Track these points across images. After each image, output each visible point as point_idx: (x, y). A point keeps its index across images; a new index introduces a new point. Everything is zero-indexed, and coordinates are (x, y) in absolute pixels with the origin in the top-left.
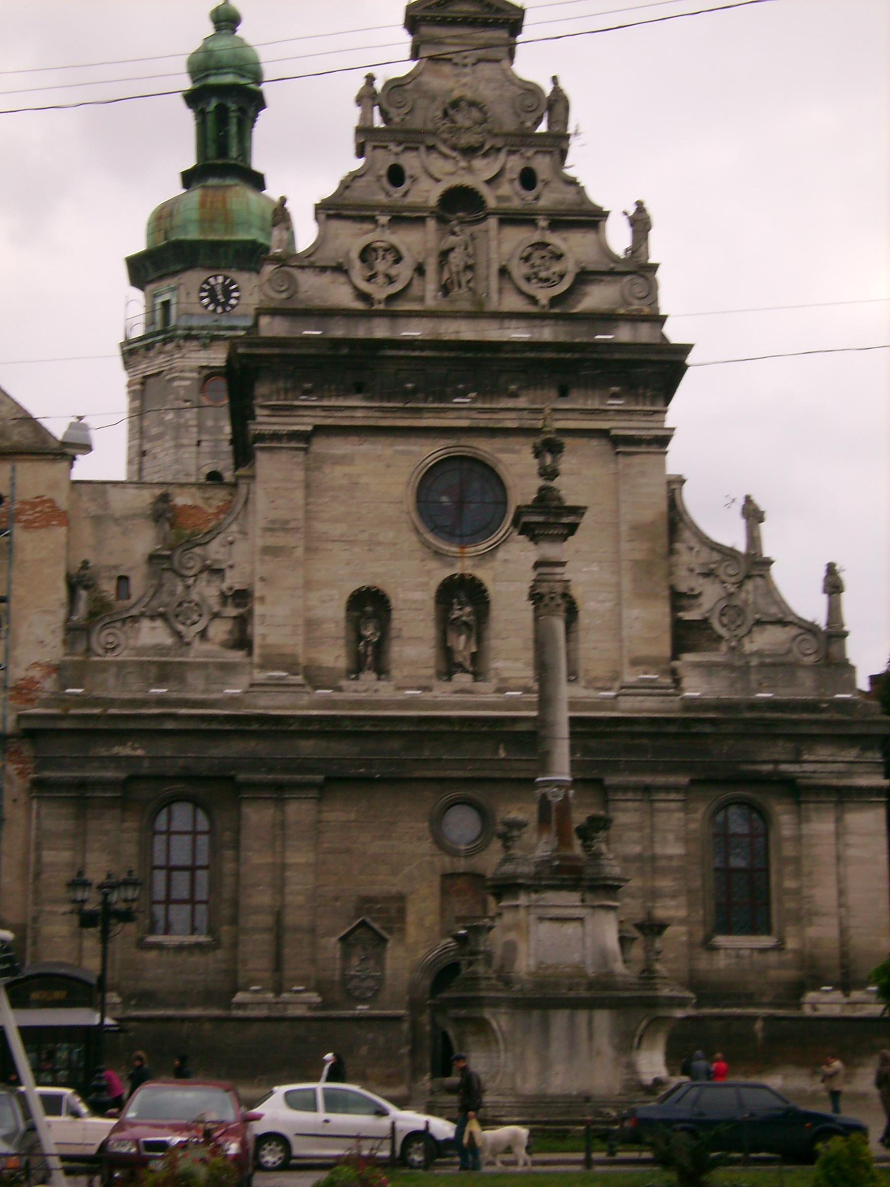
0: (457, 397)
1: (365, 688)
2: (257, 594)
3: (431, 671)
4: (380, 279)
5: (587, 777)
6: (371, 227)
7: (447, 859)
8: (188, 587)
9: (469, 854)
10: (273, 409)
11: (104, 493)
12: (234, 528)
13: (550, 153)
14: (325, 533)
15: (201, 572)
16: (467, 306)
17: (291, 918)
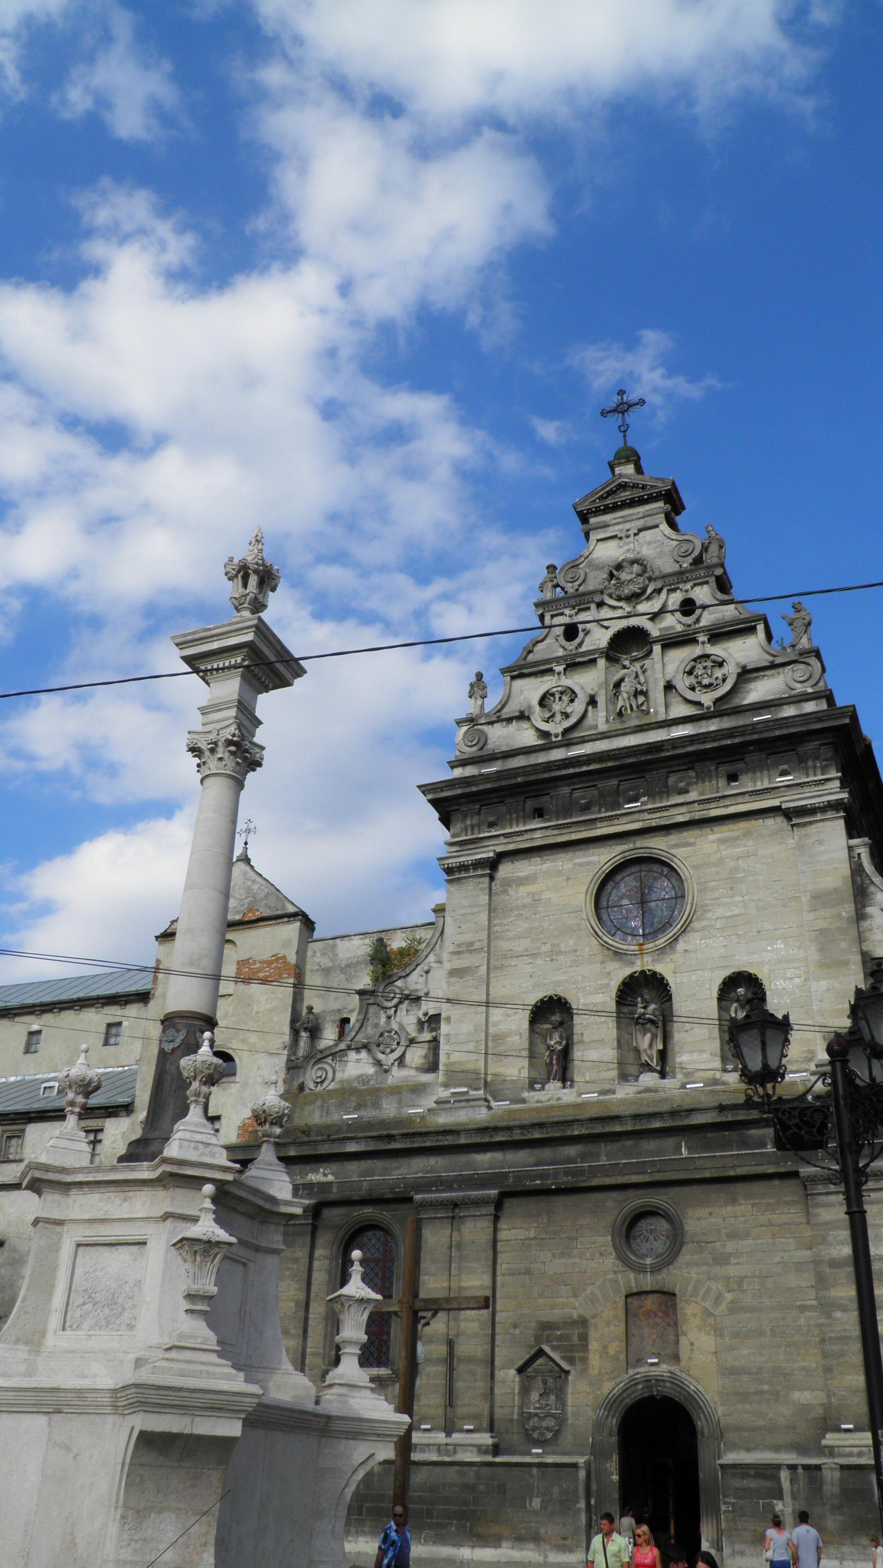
0: (628, 803)
1: (548, 1097)
2: (443, 1016)
3: (614, 1073)
4: (558, 717)
5: (782, 1170)
6: (551, 678)
7: (632, 1276)
8: (389, 1017)
9: (656, 1269)
10: (461, 845)
11: (335, 946)
12: (432, 958)
13: (707, 583)
14: (510, 950)
15: (400, 1002)
16: (637, 722)
17: (463, 1349)
